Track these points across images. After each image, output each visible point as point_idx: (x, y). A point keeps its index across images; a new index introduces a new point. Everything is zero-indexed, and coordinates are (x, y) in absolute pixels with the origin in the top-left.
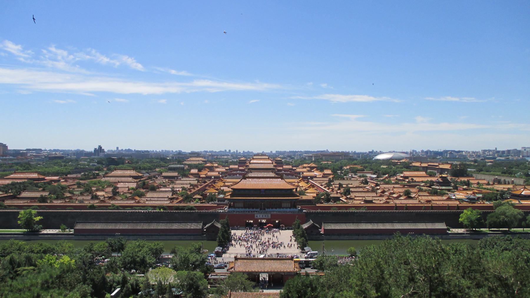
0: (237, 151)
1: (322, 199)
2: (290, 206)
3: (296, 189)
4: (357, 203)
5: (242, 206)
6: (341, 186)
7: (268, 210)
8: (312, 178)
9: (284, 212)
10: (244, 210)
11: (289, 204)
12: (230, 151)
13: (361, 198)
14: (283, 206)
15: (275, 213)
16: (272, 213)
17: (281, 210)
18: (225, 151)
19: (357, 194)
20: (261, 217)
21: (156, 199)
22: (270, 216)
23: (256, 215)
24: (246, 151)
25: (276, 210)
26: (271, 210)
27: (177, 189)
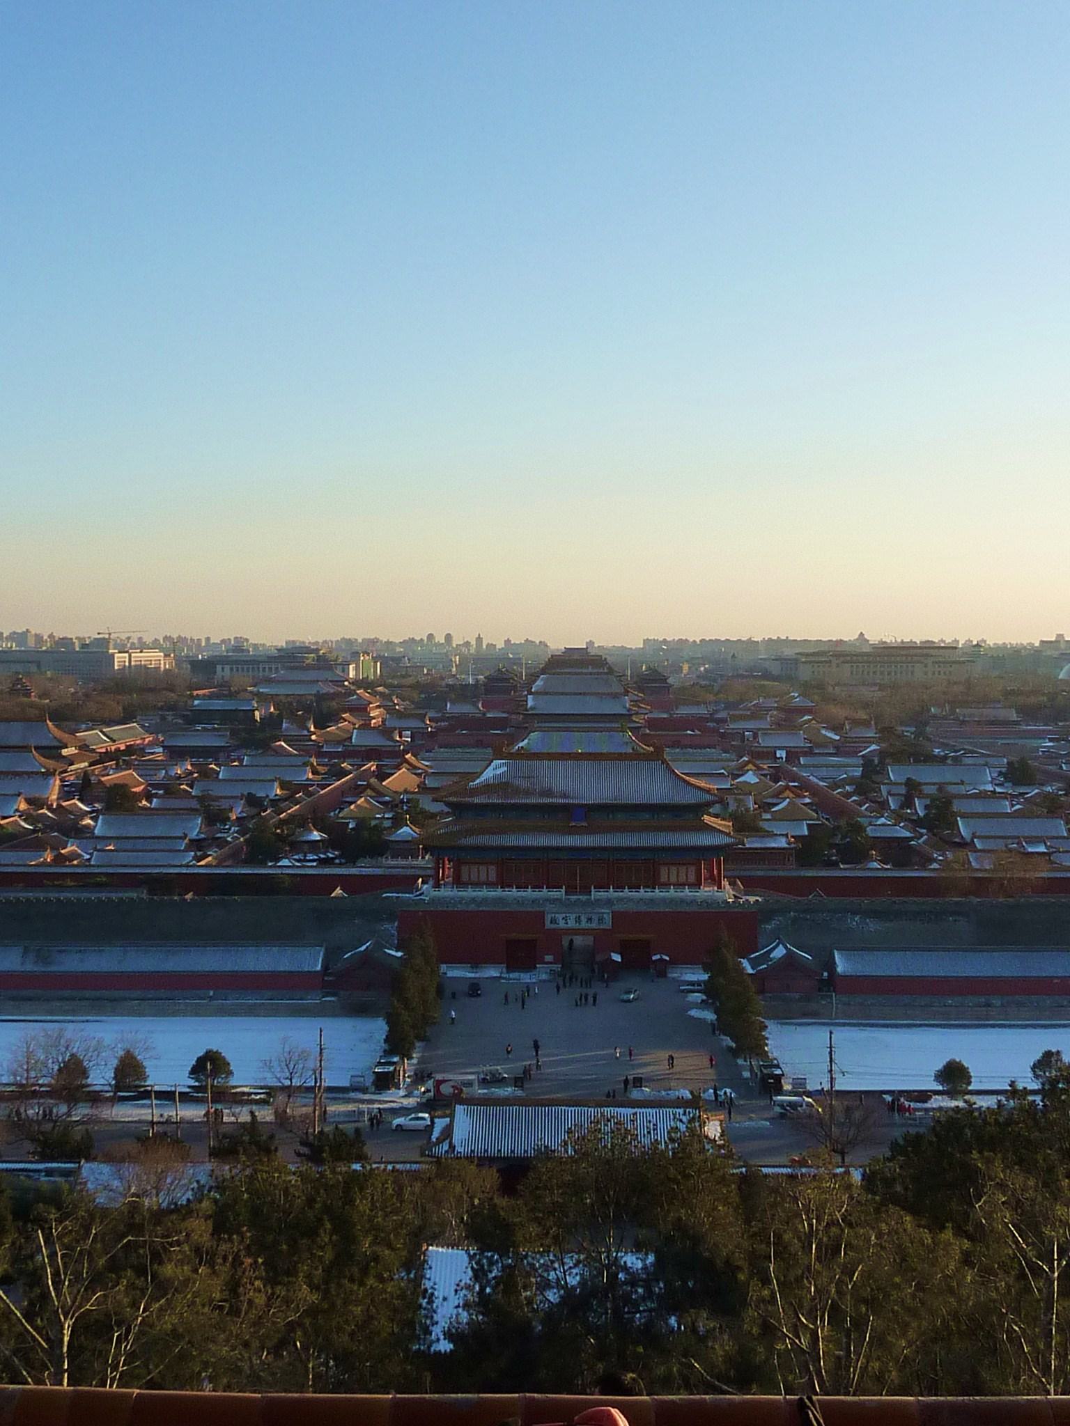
0: (479, 639)
1: (832, 846)
2: (692, 879)
3: (725, 805)
4: (980, 864)
5: (493, 876)
6: (912, 787)
7: (602, 894)
8: (792, 755)
9: (672, 900)
10: (498, 893)
11: (692, 869)
12: (449, 637)
13: (1000, 845)
14: (664, 878)
15: (631, 907)
16: (618, 907)
17: (658, 893)
18: (431, 636)
19: (984, 827)
20: (571, 924)
21: (140, 844)
22: (608, 918)
23: (548, 918)
24: (517, 639)
25: (633, 894)
26: (612, 893)
27: (225, 804)
